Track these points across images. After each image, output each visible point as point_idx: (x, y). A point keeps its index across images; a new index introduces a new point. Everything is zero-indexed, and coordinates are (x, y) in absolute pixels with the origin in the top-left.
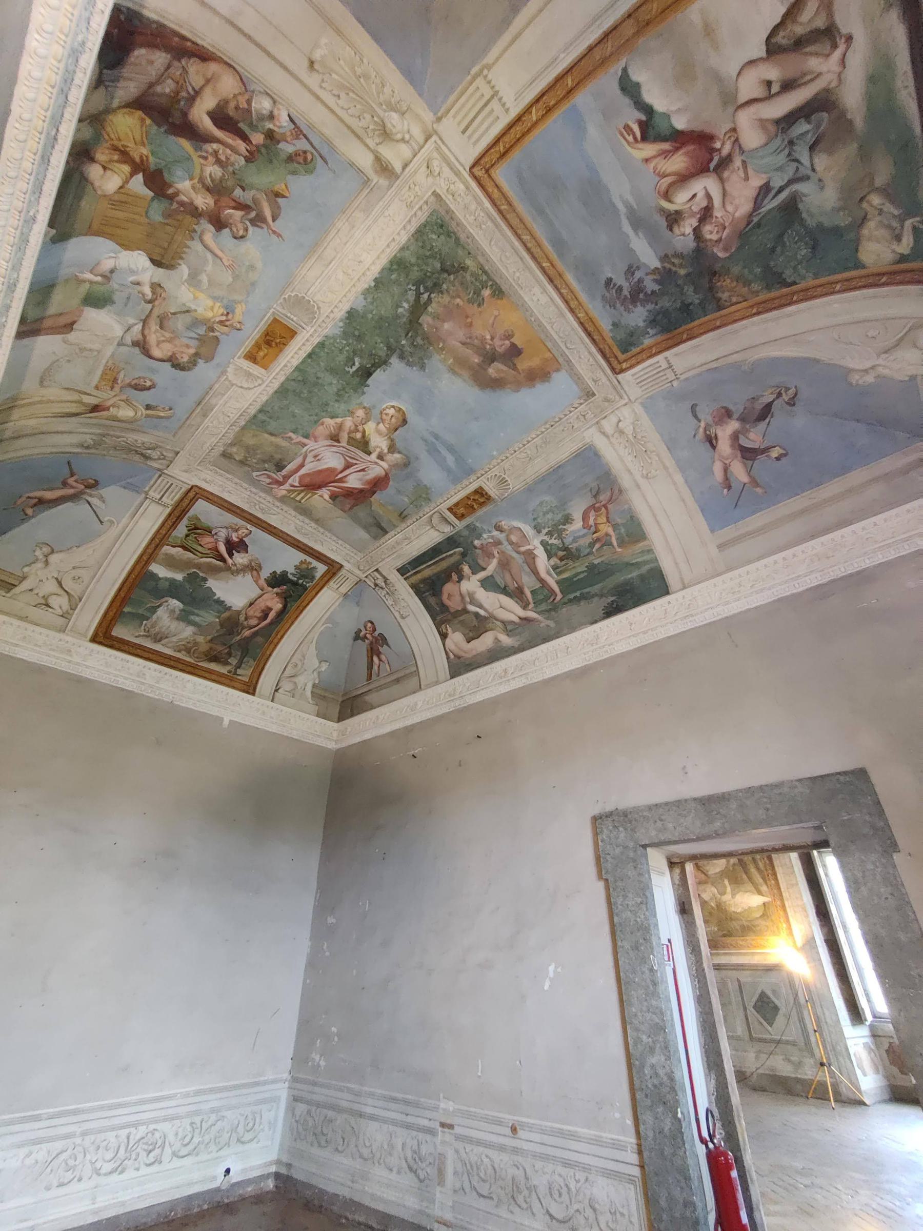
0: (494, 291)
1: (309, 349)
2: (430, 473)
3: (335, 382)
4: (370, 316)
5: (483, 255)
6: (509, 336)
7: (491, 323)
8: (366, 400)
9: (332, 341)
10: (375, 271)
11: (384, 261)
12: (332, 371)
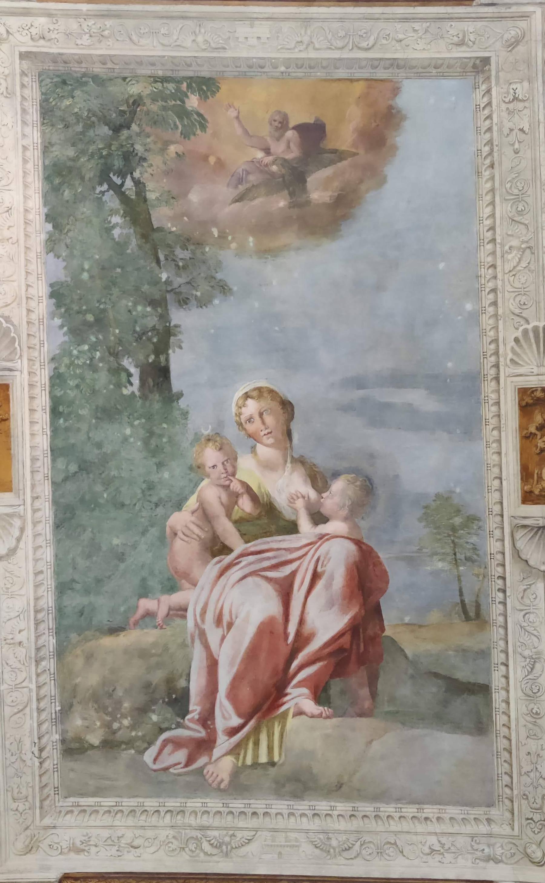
0: (200, 90)
1: (43, 400)
2: (422, 464)
3: (128, 431)
4: (85, 276)
5: (140, 63)
6: (282, 125)
7: (241, 133)
8: (200, 422)
9: (66, 361)
10: (36, 203)
11: (36, 184)
12: (107, 414)
